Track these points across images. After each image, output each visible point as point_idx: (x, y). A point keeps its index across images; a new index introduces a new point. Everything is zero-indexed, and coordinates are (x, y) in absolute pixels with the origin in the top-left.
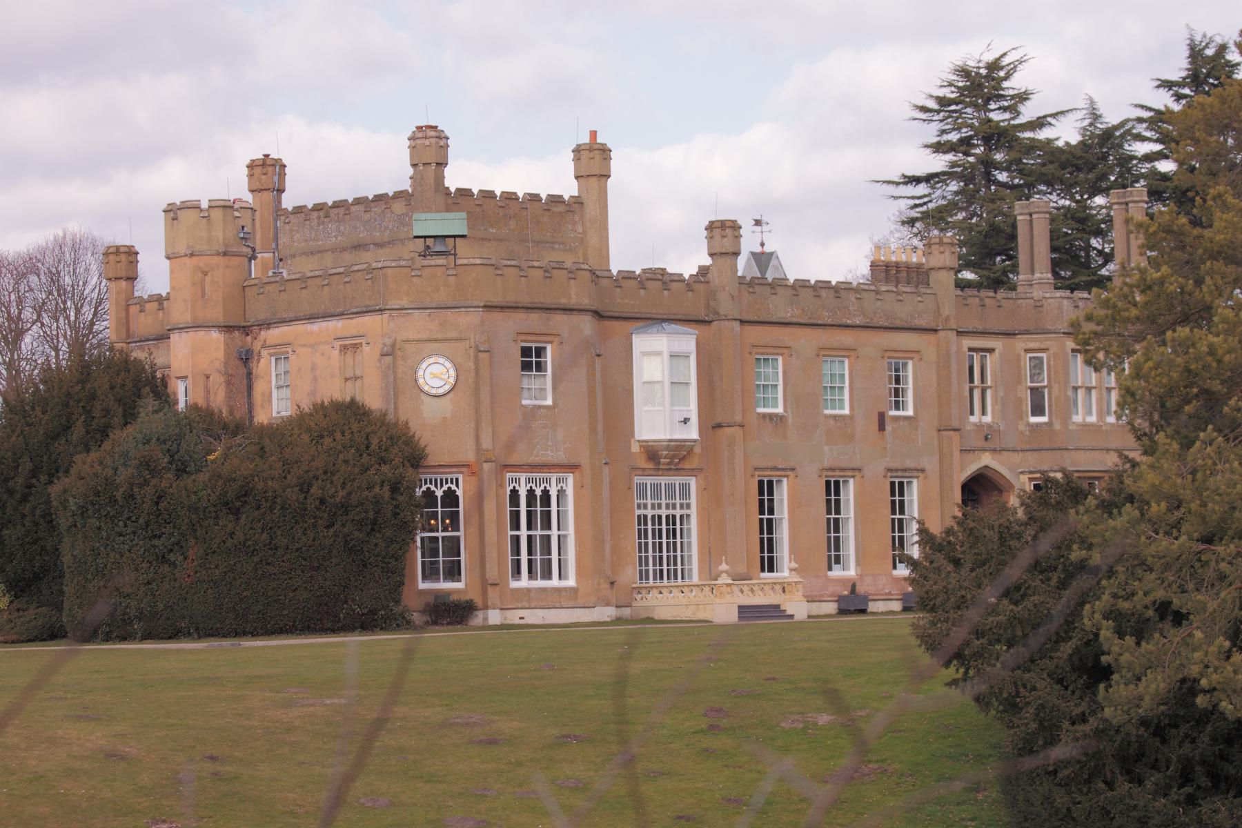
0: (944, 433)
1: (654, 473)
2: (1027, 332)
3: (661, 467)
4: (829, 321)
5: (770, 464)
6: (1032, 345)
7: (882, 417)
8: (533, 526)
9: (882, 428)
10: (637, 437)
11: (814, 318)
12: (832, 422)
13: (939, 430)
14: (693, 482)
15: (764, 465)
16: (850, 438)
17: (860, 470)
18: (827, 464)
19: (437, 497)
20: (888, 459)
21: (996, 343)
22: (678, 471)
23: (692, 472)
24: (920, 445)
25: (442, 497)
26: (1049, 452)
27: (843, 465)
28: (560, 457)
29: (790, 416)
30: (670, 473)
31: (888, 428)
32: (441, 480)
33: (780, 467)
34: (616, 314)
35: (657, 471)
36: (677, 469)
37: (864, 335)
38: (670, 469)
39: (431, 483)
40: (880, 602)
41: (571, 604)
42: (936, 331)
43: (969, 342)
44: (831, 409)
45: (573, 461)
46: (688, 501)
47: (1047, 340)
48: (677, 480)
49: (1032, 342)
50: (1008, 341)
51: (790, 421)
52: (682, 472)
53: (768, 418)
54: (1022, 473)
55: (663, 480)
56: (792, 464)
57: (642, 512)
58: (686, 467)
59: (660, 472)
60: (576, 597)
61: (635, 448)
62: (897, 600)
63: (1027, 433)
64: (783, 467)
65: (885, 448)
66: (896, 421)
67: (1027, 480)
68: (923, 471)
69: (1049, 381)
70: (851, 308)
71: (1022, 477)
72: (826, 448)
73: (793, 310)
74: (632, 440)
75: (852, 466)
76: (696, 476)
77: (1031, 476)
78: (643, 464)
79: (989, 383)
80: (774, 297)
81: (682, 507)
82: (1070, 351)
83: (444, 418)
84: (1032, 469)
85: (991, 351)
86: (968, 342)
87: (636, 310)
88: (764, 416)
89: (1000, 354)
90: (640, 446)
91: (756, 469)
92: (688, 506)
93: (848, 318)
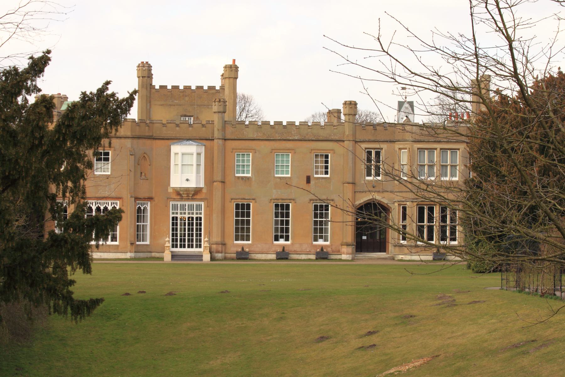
0: (345, 184)
1: (180, 200)
2: (399, 141)
3: (184, 198)
4: (279, 138)
5: (241, 197)
6: (401, 146)
8: (139, 221)
11: (270, 137)
12: (278, 180)
13: (344, 183)
14: (203, 203)
15: (237, 197)
17: (294, 200)
18: (274, 197)
19: (101, 209)
22: (193, 199)
23: (201, 200)
25: (103, 209)
27: (283, 198)
28: (113, 195)
29: (254, 178)
30: (190, 200)
31: (312, 182)
32: (103, 203)
33: (246, 198)
34: (161, 138)
35: (182, 199)
36: (192, 199)
37: (299, 143)
38: (189, 199)
39: (115, 204)
40: (304, 255)
41: (116, 251)
42: (344, 141)
43: (365, 145)
45: (119, 196)
47: (406, 144)
48: (195, 203)
49: (401, 145)
50: (392, 145)
51: (253, 180)
52: (195, 200)
53: (240, 179)
55: (187, 203)
56: (253, 197)
58: (198, 198)
59: (184, 200)
60: (118, 249)
61: (170, 190)
62: (314, 254)
64: (248, 198)
66: (317, 179)
72: (274, 191)
73: (258, 134)
74: (169, 187)
76: (204, 201)
77: (399, 203)
80: (247, 129)
81: (197, 214)
82: (416, 149)
84: (399, 200)
86: (364, 146)
87: (174, 136)
88: (239, 177)
89: (385, 150)
90: (173, 190)
91: (232, 199)
92: (201, 214)
93: (291, 137)
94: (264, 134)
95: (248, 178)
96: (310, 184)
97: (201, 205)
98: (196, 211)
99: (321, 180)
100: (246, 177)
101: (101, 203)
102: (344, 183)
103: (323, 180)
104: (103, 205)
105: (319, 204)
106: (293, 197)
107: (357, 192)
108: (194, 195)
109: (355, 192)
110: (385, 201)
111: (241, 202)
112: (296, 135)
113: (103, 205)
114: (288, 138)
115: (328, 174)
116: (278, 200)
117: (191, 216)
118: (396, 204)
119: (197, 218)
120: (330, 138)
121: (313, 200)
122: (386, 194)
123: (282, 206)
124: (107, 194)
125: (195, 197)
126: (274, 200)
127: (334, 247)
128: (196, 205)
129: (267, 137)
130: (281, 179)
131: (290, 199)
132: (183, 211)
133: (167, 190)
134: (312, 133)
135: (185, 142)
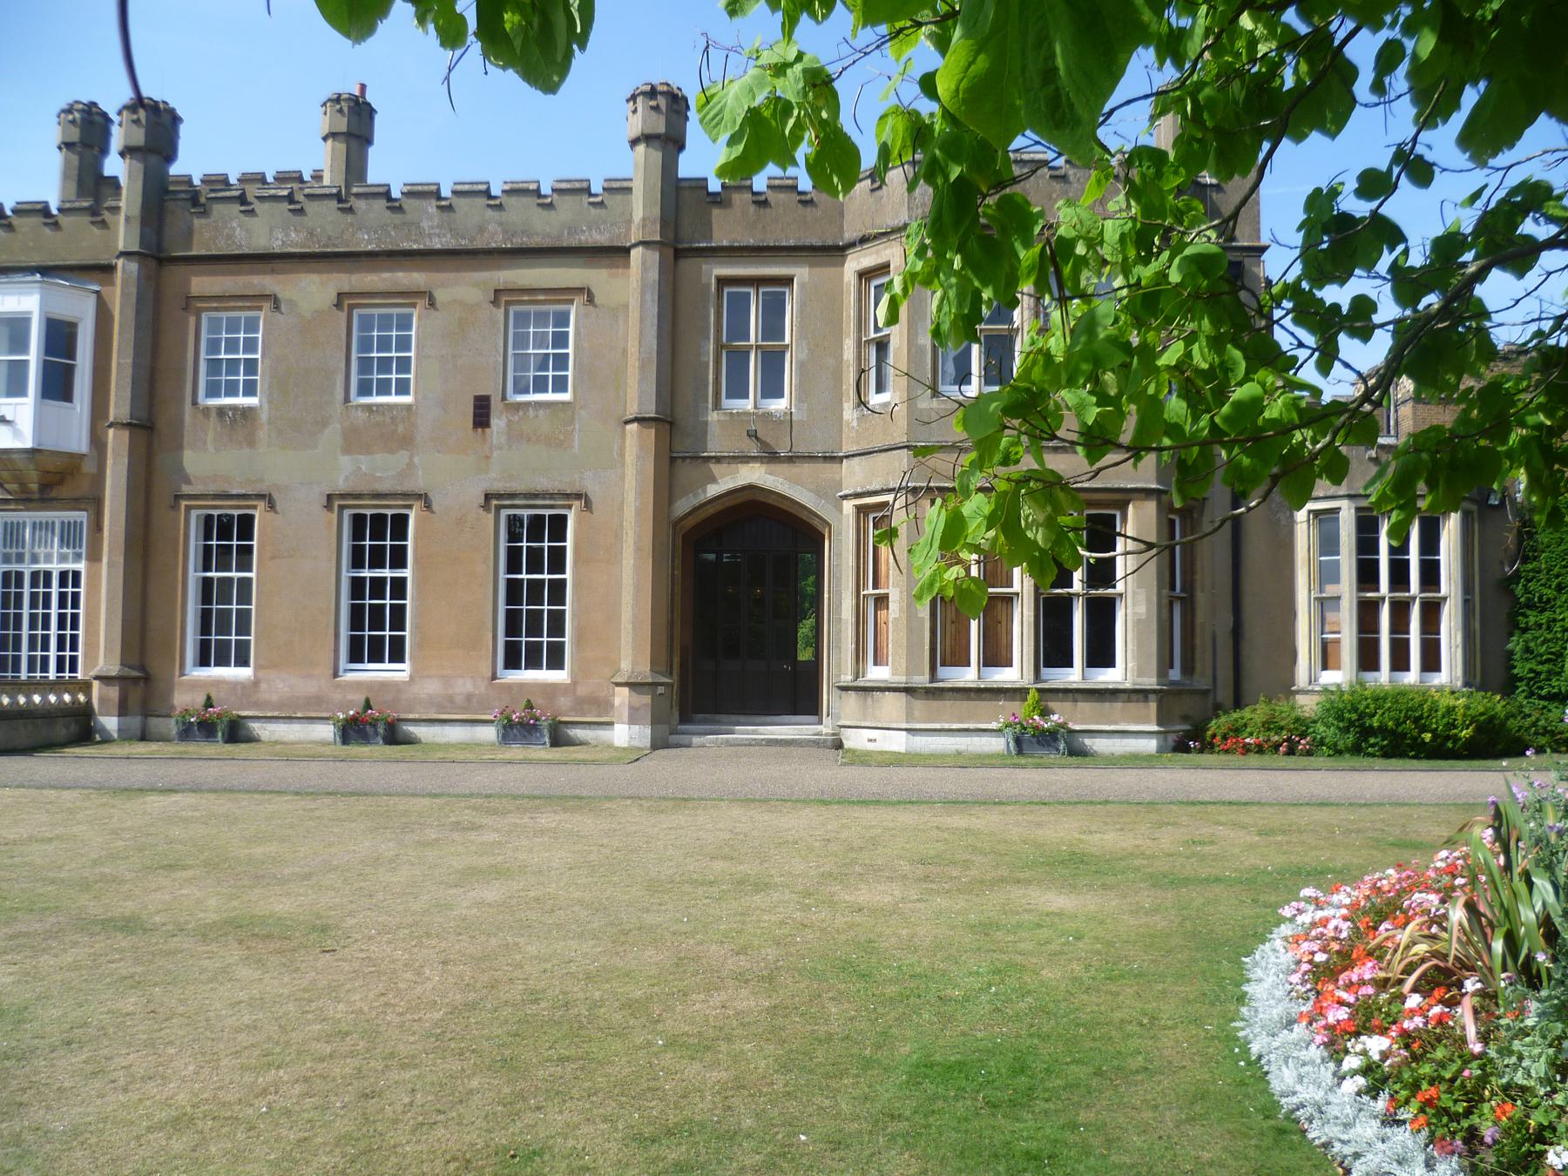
16: (407, 442)
18: (342, 485)
21: (801, 273)
24: (576, 450)
26: (883, 454)
29: (266, 407)
30: (32, 505)
31: (498, 422)
33: (234, 492)
38: (30, 500)
44: (397, 393)
46: (20, 550)
51: (264, 416)
53: (213, 414)
54: (845, 497)
57: (14, 567)
63: (855, 424)
65: (488, 458)
68: (578, 496)
70: (425, 224)
72: (345, 461)
75: (408, 486)
79: (787, 340)
81: (63, 558)
84: (859, 490)
85: (788, 281)
88: (207, 409)
89: (802, 286)
93: (415, 241)
94: (311, 234)
95: (246, 413)
96: (487, 430)
99: (531, 413)
100: (234, 408)
103: (541, 412)
105: (526, 513)
106: (418, 483)
107: (684, 458)
108: (45, 487)
109: (673, 460)
110: (802, 495)
111: (215, 507)
114: (406, 245)
115: (565, 390)
116: (358, 496)
117: (42, 566)
118: (849, 507)
119: (63, 576)
120: (574, 242)
121: (499, 496)
122: (805, 469)
123: (379, 520)
125: (54, 494)
126: (343, 496)
127: (582, 691)
128: (63, 523)
129: (324, 246)
131: (406, 495)
134: (501, 224)
135: (18, 278)
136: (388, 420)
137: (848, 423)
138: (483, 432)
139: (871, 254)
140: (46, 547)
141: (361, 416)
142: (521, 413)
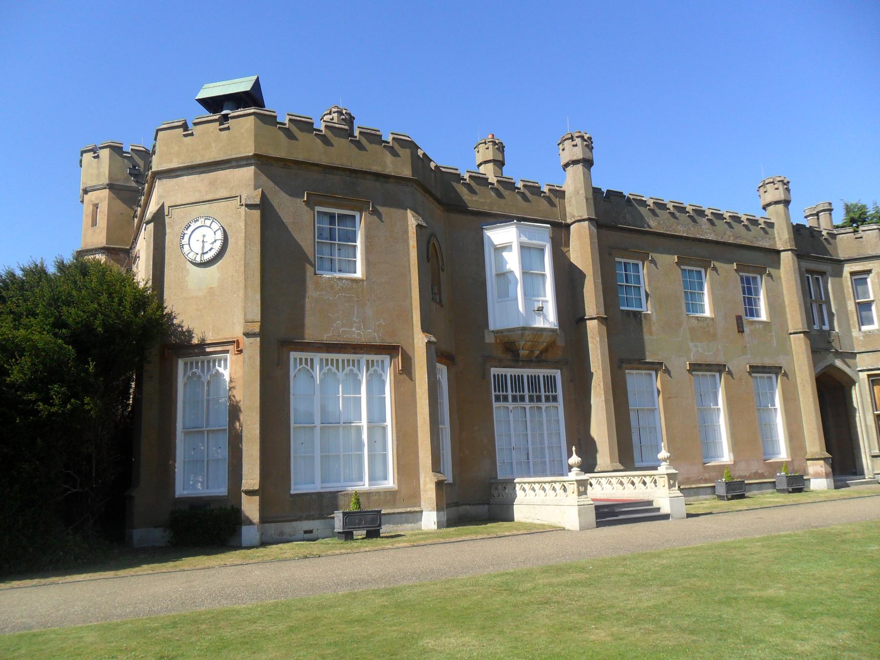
7: (739, 319)
9: (741, 330)
10: (492, 326)
14: (557, 374)
20: (749, 356)
23: (555, 365)
31: (747, 329)
45: (389, 341)
48: (541, 372)
51: (654, 318)
53: (632, 316)
55: (526, 372)
61: (490, 339)
63: (861, 338)
67: (866, 376)
69: (875, 296)
71: (860, 373)
72: (691, 345)
78: (499, 353)
83: (210, 288)
90: (496, 338)
97: (554, 376)
98: (545, 392)
101: (337, 361)
102: (791, 334)
104: (343, 369)
112: (709, 233)
113: (343, 369)
117: (535, 404)
124: (357, 334)
130: (698, 320)
132: (535, 394)
133: (483, 338)
136: (706, 325)
137: (857, 338)
138: (742, 335)
139: (860, 265)
140: (552, 392)
141: (695, 322)
142: (753, 326)
